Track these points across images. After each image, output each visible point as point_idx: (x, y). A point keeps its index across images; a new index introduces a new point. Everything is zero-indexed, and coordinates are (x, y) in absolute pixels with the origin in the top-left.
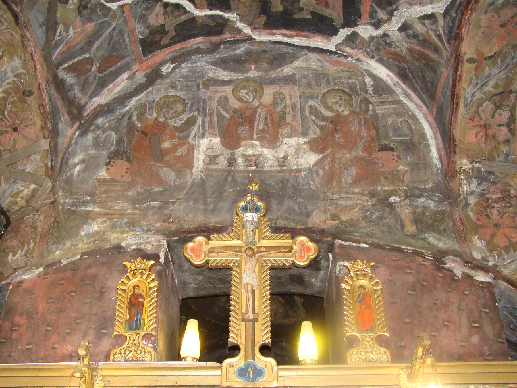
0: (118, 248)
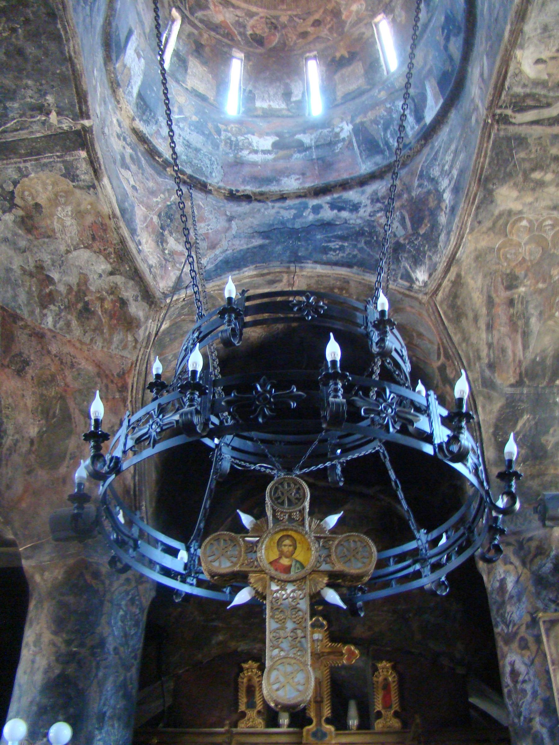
0: (235, 652)
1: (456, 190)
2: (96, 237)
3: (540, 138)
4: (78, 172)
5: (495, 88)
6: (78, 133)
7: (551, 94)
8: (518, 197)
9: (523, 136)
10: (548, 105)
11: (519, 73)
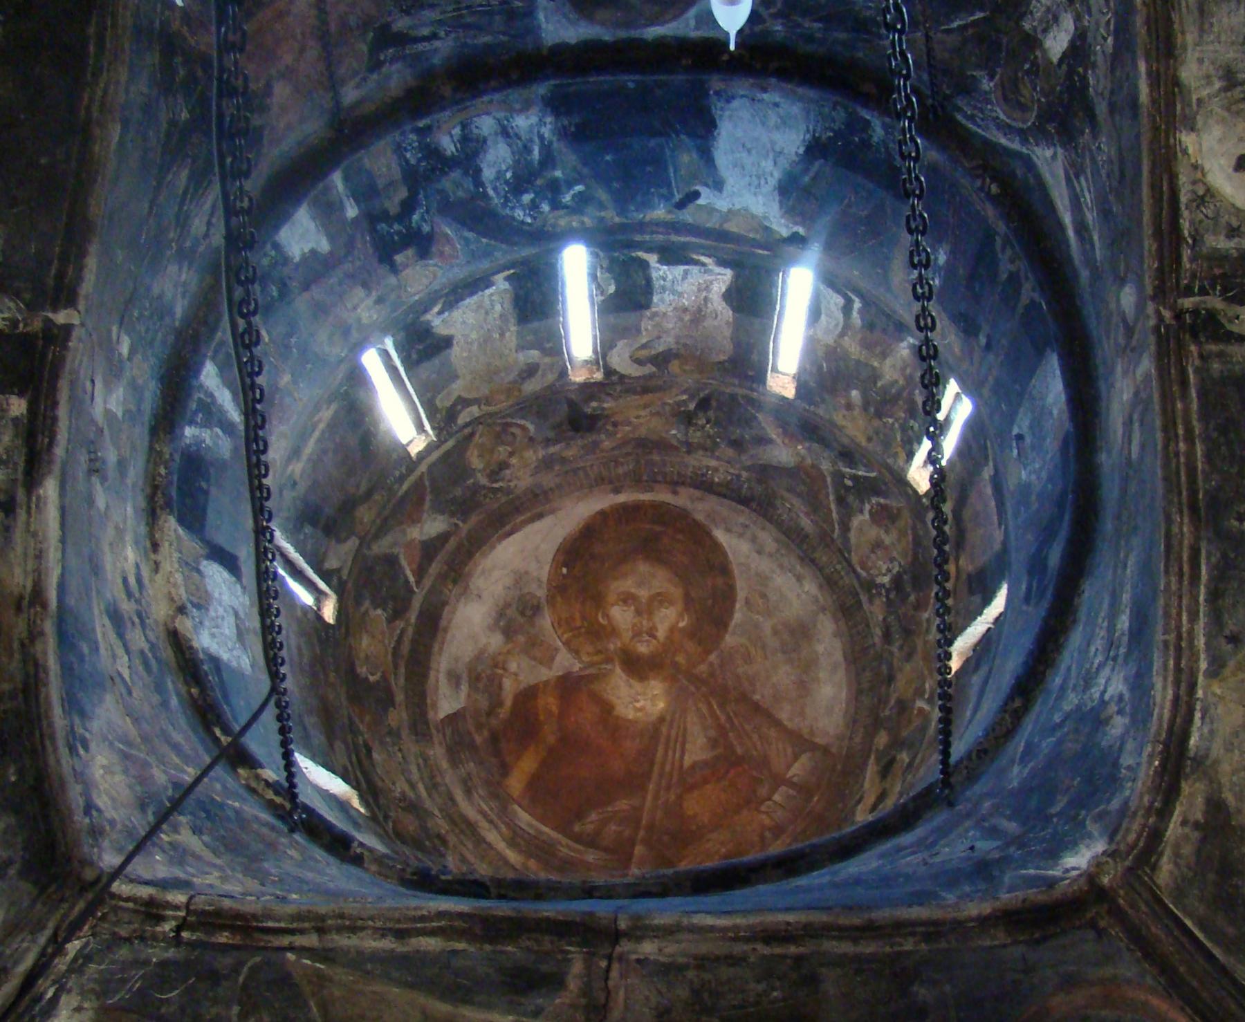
5: (1158, 234)
11: (1206, 196)
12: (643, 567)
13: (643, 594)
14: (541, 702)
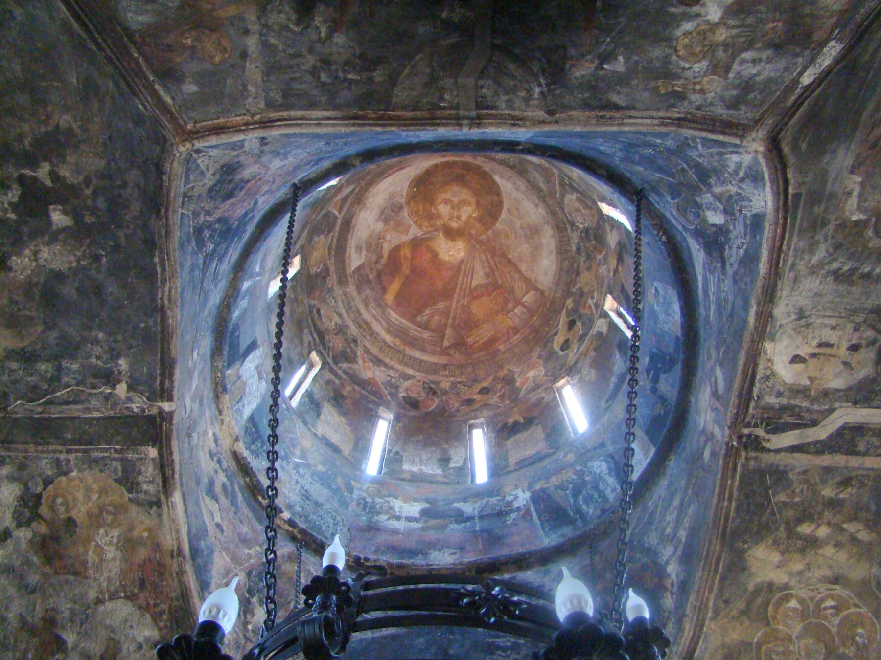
1: (687, 558)
2: (147, 583)
3: (805, 472)
4: (140, 478)
5: (740, 395)
6: (151, 419)
7: (816, 407)
8: (780, 562)
9: (781, 468)
10: (814, 423)
11: (771, 375)
12: (456, 188)
13: (456, 200)
14: (402, 253)
